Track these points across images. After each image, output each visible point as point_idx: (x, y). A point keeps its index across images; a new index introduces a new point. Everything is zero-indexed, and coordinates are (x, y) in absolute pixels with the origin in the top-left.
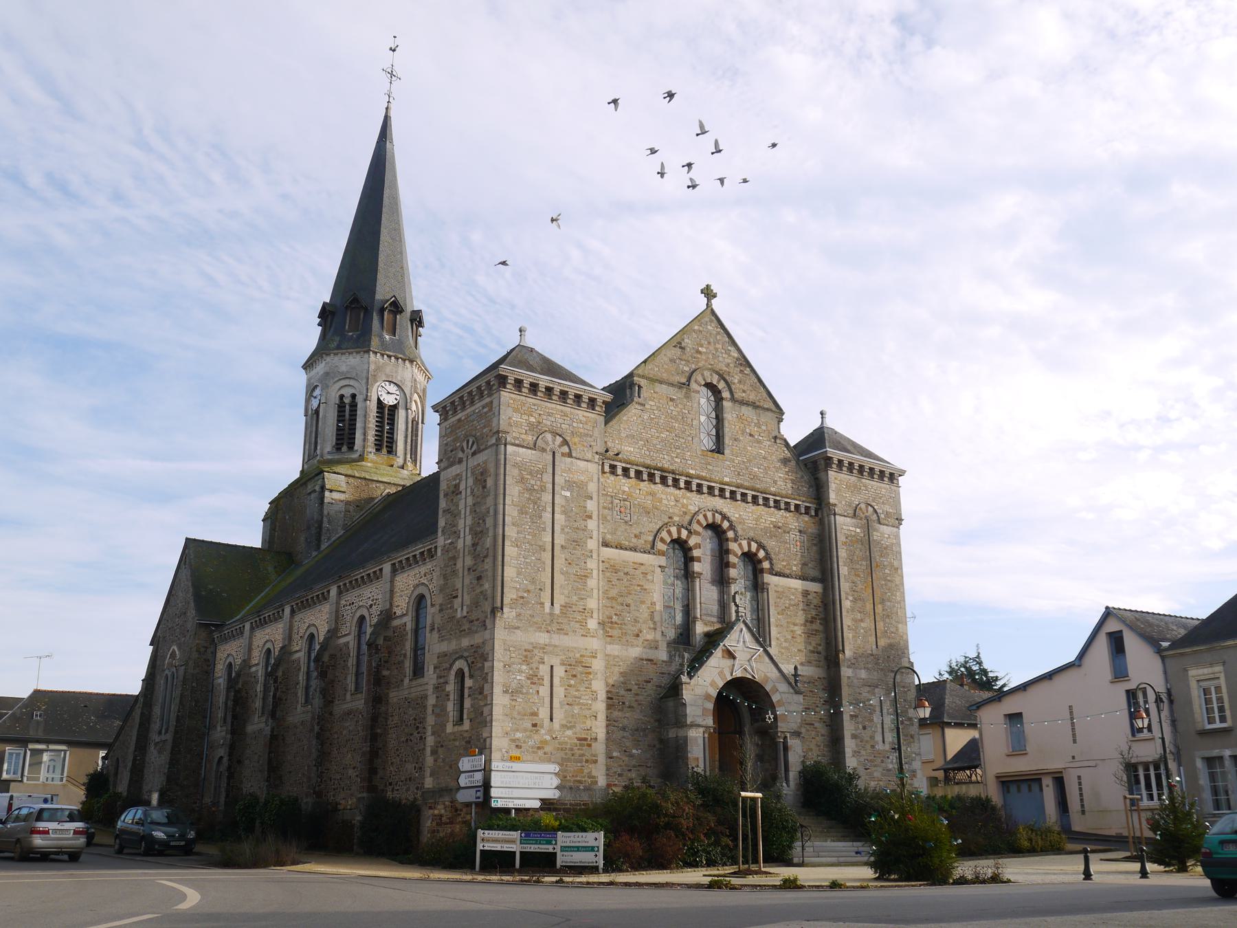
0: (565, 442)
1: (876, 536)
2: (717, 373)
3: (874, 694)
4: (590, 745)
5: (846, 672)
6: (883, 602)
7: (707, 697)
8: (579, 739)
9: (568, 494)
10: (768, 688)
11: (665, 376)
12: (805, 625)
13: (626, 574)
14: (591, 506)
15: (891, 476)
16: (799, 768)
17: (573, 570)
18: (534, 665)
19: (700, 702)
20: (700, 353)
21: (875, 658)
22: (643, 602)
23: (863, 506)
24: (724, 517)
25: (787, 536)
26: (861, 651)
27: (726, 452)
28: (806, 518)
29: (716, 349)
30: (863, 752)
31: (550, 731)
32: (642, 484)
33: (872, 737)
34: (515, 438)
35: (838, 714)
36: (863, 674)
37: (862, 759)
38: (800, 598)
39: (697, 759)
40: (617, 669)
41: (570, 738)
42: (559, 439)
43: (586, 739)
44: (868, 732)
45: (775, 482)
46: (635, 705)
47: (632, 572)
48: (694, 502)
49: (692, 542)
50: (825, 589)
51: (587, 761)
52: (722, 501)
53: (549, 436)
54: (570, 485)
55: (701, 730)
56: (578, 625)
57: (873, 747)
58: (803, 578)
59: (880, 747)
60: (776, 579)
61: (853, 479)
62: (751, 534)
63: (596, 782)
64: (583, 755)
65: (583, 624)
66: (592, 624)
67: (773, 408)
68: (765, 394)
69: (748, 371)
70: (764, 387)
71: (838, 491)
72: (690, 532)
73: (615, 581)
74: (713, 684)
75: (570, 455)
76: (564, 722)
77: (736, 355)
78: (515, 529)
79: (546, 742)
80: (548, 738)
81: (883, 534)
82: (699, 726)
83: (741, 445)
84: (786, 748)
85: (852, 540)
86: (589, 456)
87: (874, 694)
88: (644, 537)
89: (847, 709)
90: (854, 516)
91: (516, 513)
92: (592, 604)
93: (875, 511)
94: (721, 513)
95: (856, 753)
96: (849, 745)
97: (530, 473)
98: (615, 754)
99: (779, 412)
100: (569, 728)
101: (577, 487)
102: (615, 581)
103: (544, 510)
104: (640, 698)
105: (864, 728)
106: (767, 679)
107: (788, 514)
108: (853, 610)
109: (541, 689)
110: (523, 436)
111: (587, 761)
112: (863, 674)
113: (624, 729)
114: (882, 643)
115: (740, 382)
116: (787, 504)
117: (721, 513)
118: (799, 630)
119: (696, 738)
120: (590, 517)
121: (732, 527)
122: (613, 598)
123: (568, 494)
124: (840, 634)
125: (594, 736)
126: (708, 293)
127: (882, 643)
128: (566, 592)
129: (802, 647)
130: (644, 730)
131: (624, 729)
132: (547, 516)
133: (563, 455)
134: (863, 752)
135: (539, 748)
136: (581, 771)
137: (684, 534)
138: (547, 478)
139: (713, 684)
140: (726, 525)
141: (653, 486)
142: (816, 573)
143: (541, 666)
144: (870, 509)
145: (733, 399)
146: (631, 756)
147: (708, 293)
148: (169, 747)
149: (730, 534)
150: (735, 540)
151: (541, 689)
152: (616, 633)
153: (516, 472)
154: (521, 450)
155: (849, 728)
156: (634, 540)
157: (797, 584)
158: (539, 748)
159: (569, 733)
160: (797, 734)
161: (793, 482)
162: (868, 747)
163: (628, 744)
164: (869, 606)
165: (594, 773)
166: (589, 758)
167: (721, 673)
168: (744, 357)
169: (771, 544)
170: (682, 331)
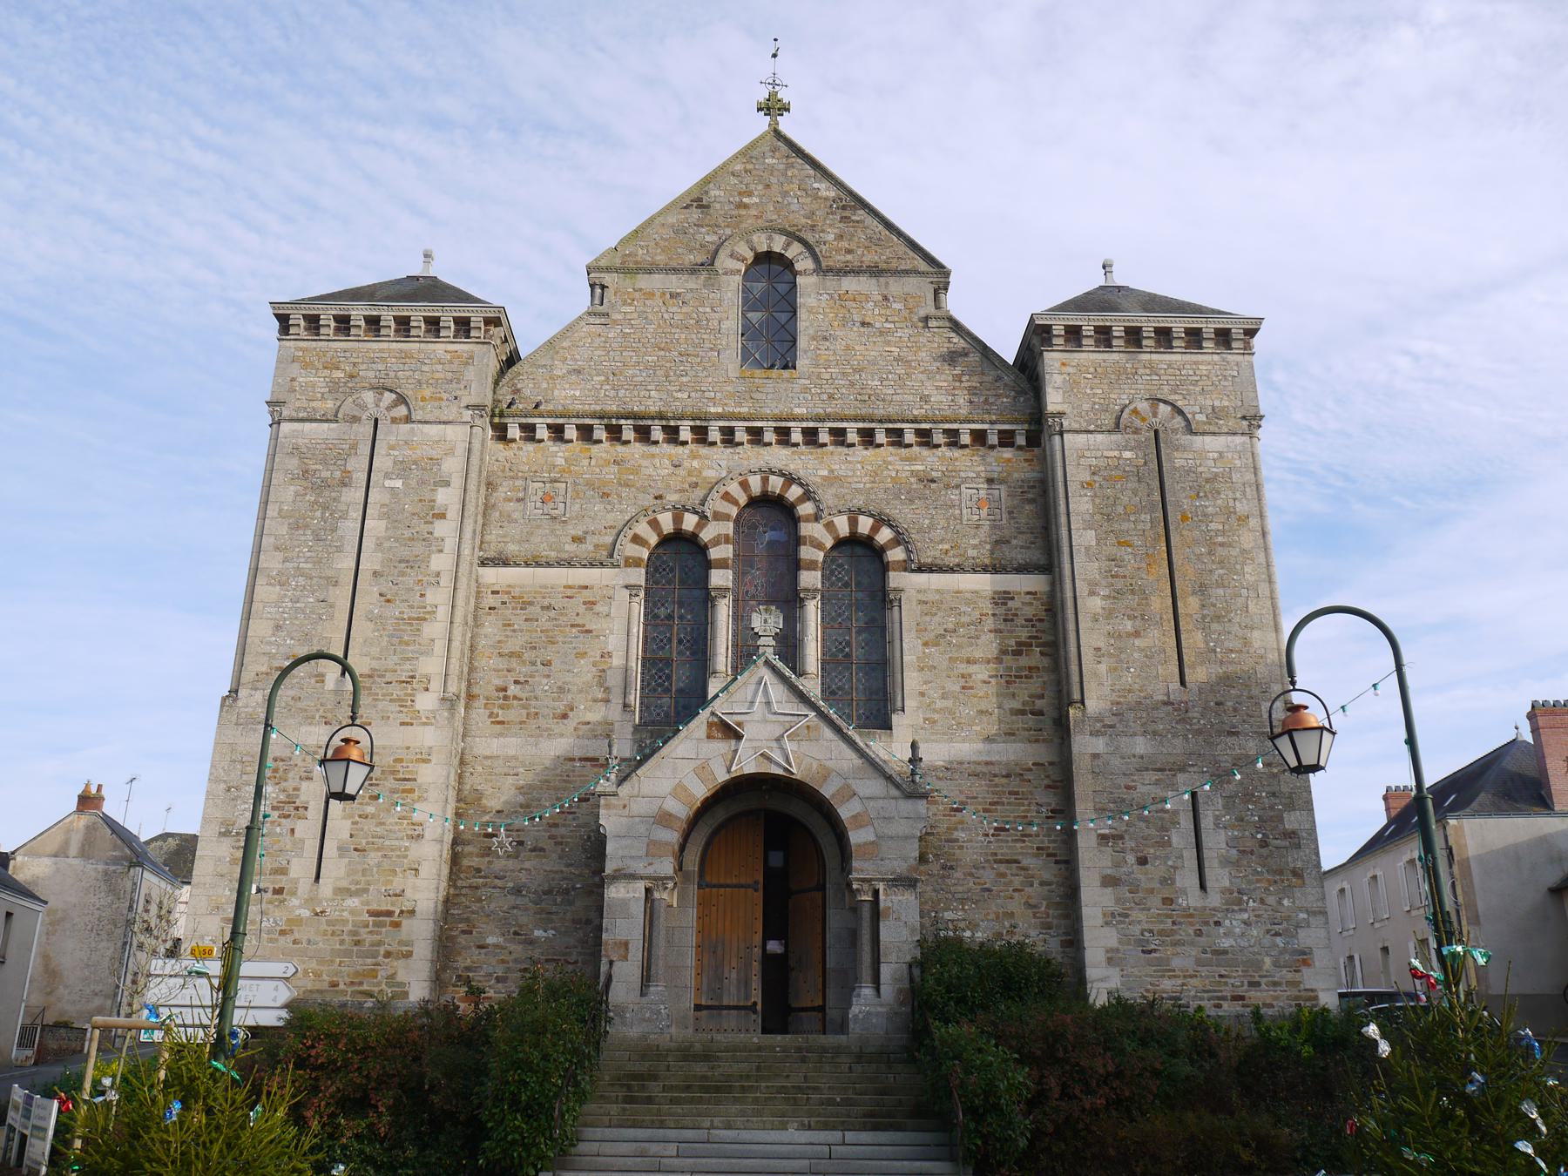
0: (402, 400)
1: (1177, 460)
2: (783, 232)
3: (1173, 786)
4: (397, 925)
5: (1084, 745)
6: (1202, 589)
7: (664, 819)
8: (372, 914)
9: (399, 484)
10: (827, 791)
11: (661, 258)
12: (999, 660)
13: (549, 608)
14: (447, 497)
15: (1233, 336)
16: (910, 953)
17: (394, 611)
18: (289, 785)
19: (642, 829)
20: (746, 206)
21: (1179, 711)
22: (583, 655)
23: (1143, 406)
24: (790, 479)
25: (953, 496)
26: (1131, 698)
27: (802, 362)
28: (1007, 453)
29: (785, 194)
30: (1136, 915)
31: (311, 901)
32: (595, 449)
33: (1167, 881)
34: (298, 410)
35: (1070, 837)
36: (1141, 746)
37: (1136, 930)
38: (988, 608)
39: (626, 944)
40: (510, 780)
41: (352, 912)
42: (389, 397)
43: (389, 913)
44: (1156, 870)
45: (925, 399)
46: (548, 845)
47: (557, 602)
48: (716, 462)
49: (706, 535)
50: (1053, 584)
51: (388, 955)
52: (784, 452)
53: (369, 397)
54: (402, 469)
55: (640, 886)
56: (394, 707)
57: (1168, 901)
58: (994, 569)
59: (1192, 899)
60: (922, 579)
61: (1114, 357)
62: (859, 502)
63: (406, 994)
64: (380, 943)
65: (406, 703)
66: (426, 702)
67: (923, 266)
68: (902, 249)
69: (861, 214)
70: (900, 234)
71: (1071, 387)
72: (703, 517)
73: (518, 623)
74: (679, 791)
75: (408, 419)
76: (344, 884)
77: (831, 193)
78: (280, 556)
79: (298, 921)
80: (305, 913)
81: (1202, 454)
82: (633, 877)
83: (839, 346)
84: (876, 914)
85: (1105, 476)
86: (451, 412)
87: (1173, 786)
88: (591, 541)
89: (1088, 828)
90: (1117, 427)
91: (284, 530)
92: (431, 666)
93: (1180, 412)
94: (781, 474)
95: (1110, 919)
96: (1095, 901)
97: (324, 462)
98: (491, 940)
99: (939, 275)
100: (351, 894)
101: (425, 473)
102: (518, 623)
103: (344, 516)
104: (562, 830)
105: (1143, 861)
106: (826, 774)
107: (957, 453)
108: (1109, 614)
109: (300, 827)
110: (314, 404)
111: (388, 955)
112: (1141, 746)
113: (517, 891)
114: (1199, 674)
115: (840, 237)
116: (956, 433)
117: (781, 474)
118: (981, 673)
119: (624, 903)
120: (442, 516)
121: (808, 496)
122: (511, 654)
123: (399, 484)
124: (1074, 668)
125: (407, 906)
126: (773, 107)
127: (1199, 674)
128: (375, 651)
129: (991, 704)
130: (567, 891)
131: (517, 891)
132: (350, 527)
133: (394, 420)
134: (1136, 915)
135: (282, 933)
136: (373, 974)
137: (689, 522)
138: (358, 465)
139: (679, 791)
140: (794, 492)
141: (620, 448)
142: (1035, 555)
143: (305, 785)
144: (1164, 409)
145: (821, 270)
146: (531, 942)
147: (773, 107)
148: (761, 886)
149: (806, 509)
150: (817, 518)
151: (300, 827)
152: (514, 714)
153: (293, 463)
154: (307, 425)
155: (1092, 862)
156: (571, 548)
157: (983, 583)
158: (282, 933)
159: (354, 902)
160: (906, 882)
161: (972, 391)
162: (1155, 901)
163: (524, 920)
164: (1160, 603)
165: (401, 977)
166: (394, 948)
167: (702, 770)
168: (851, 193)
169: (903, 513)
170: (707, 181)
